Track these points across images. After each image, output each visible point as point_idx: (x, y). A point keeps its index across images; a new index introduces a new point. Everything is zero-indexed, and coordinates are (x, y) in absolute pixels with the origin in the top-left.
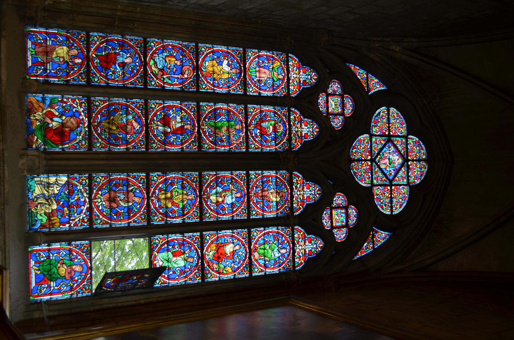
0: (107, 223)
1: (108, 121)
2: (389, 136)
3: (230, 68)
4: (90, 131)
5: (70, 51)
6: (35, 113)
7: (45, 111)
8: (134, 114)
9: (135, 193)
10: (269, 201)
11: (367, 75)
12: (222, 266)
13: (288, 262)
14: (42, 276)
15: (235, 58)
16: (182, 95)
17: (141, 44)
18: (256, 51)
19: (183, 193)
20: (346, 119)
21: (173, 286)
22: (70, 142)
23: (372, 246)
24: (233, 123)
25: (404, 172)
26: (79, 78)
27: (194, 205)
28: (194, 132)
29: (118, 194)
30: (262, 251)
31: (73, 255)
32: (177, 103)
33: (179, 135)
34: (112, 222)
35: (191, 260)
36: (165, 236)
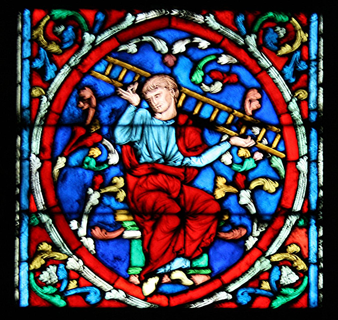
17: (59, 22)
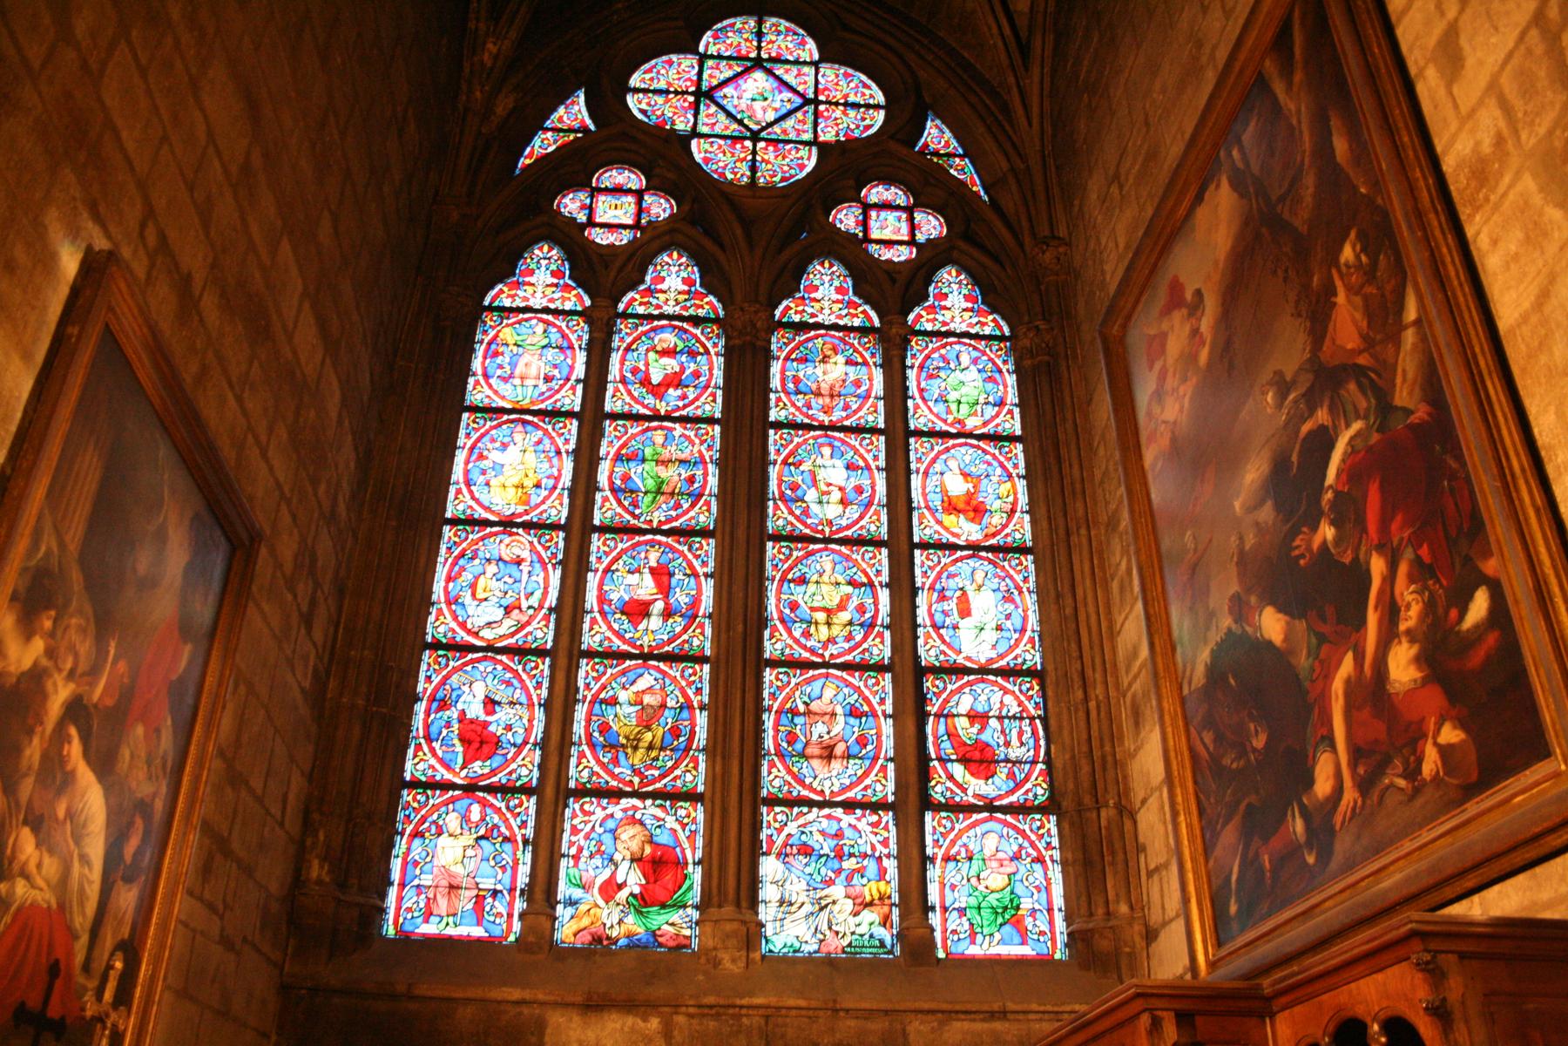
0: (884, 769)
4: (654, 795)
7: (601, 902)
9: (813, 696)
11: (547, 130)
12: (997, 504)
14: (1008, 928)
15: (487, 432)
16: (575, 567)
18: (471, 380)
21: (1041, 621)
24: (648, 452)
25: (787, 71)
28: (667, 545)
29: (815, 737)
30: (965, 409)
31: (958, 853)
32: (592, 580)
33: (674, 581)
35: (979, 576)
36: (920, 631)
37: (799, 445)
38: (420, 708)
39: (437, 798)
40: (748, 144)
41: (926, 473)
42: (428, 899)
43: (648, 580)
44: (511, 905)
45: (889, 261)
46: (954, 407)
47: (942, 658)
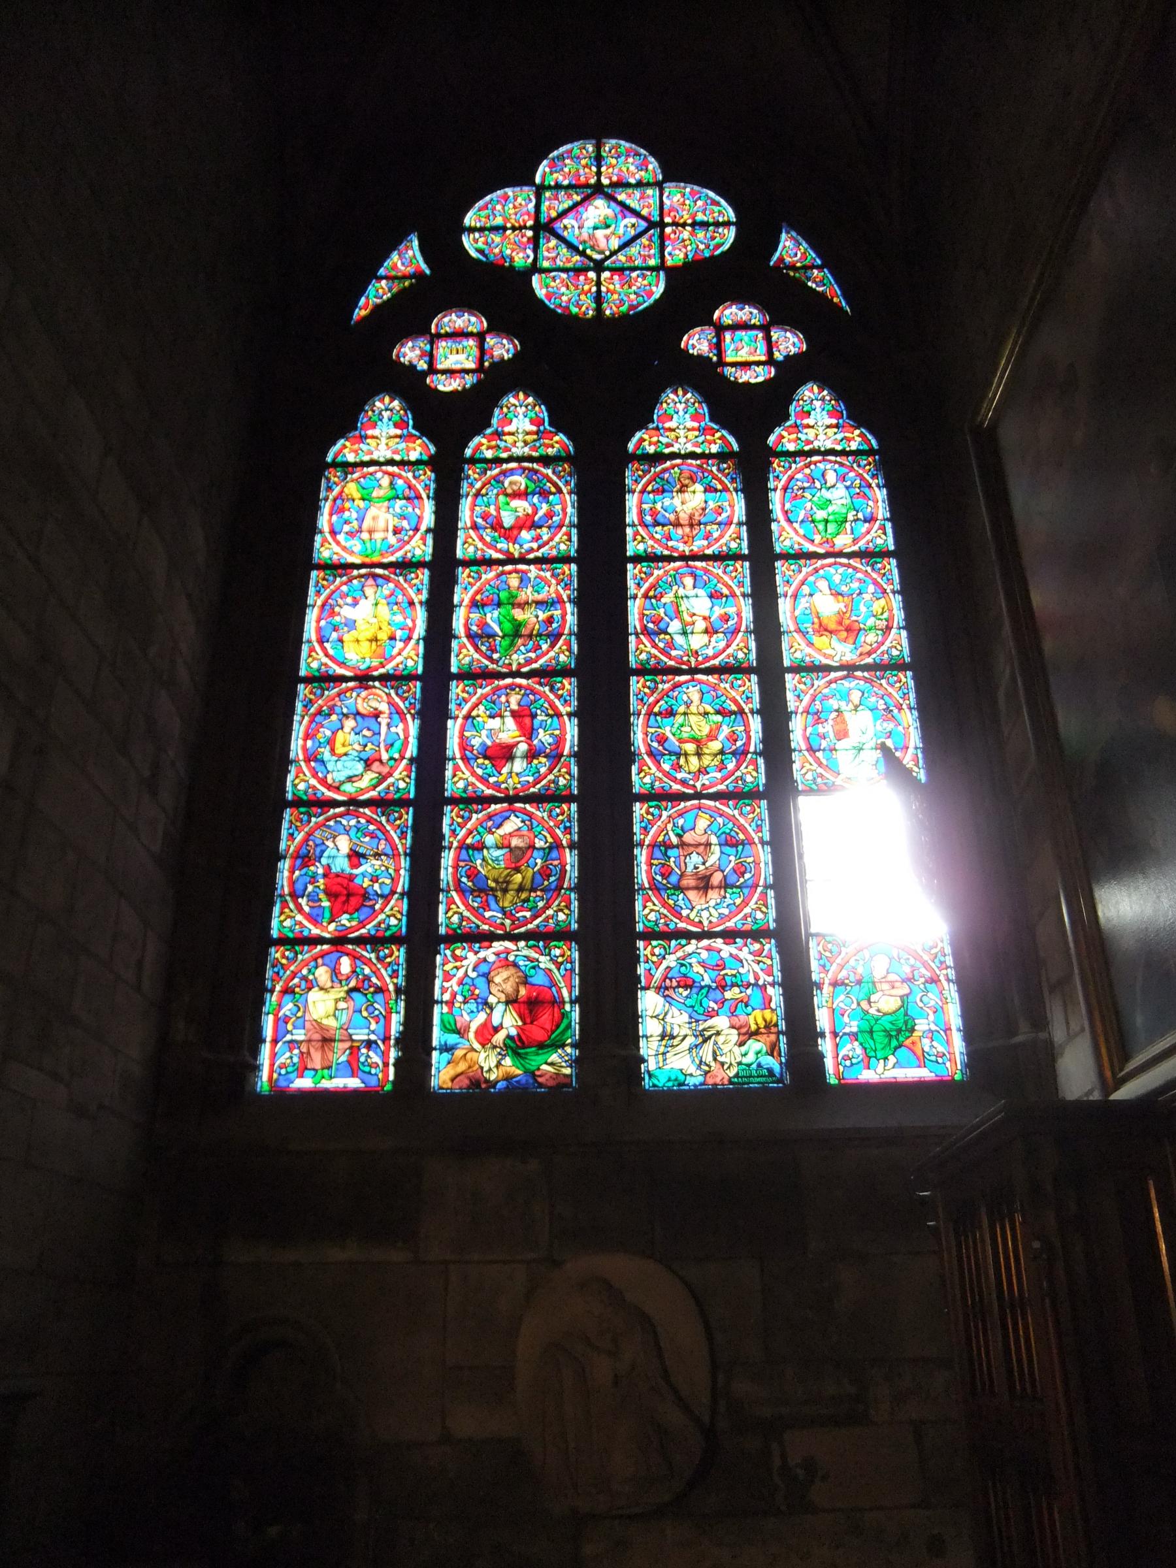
0: (764, 896)
1: (499, 894)
2: (538, 227)
3: (363, 602)
4: (526, 937)
5: (321, 984)
6: (482, 1068)
7: (477, 1046)
8: (480, 829)
9: (687, 827)
10: (704, 509)
12: (871, 622)
13: (859, 466)
14: (903, 1051)
15: (338, 588)
19: (685, 714)
20: (494, 328)
22: (556, 985)
23: (815, 272)
26: (389, 964)
27: (715, 688)
28: (527, 688)
29: (690, 869)
30: (832, 528)
32: (453, 728)
33: (536, 723)
34: (761, 883)
37: (659, 578)
38: (284, 866)
39: (306, 954)
40: (592, 275)
41: (795, 596)
42: (302, 1053)
43: (510, 722)
44: (385, 1055)
45: (747, 384)
46: (821, 527)
47: (819, 780)
